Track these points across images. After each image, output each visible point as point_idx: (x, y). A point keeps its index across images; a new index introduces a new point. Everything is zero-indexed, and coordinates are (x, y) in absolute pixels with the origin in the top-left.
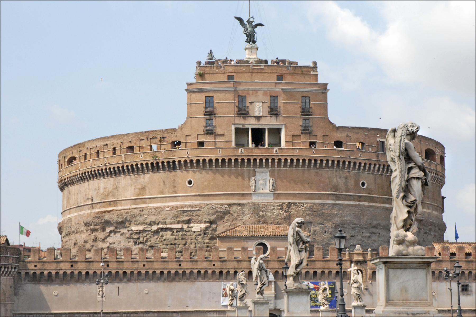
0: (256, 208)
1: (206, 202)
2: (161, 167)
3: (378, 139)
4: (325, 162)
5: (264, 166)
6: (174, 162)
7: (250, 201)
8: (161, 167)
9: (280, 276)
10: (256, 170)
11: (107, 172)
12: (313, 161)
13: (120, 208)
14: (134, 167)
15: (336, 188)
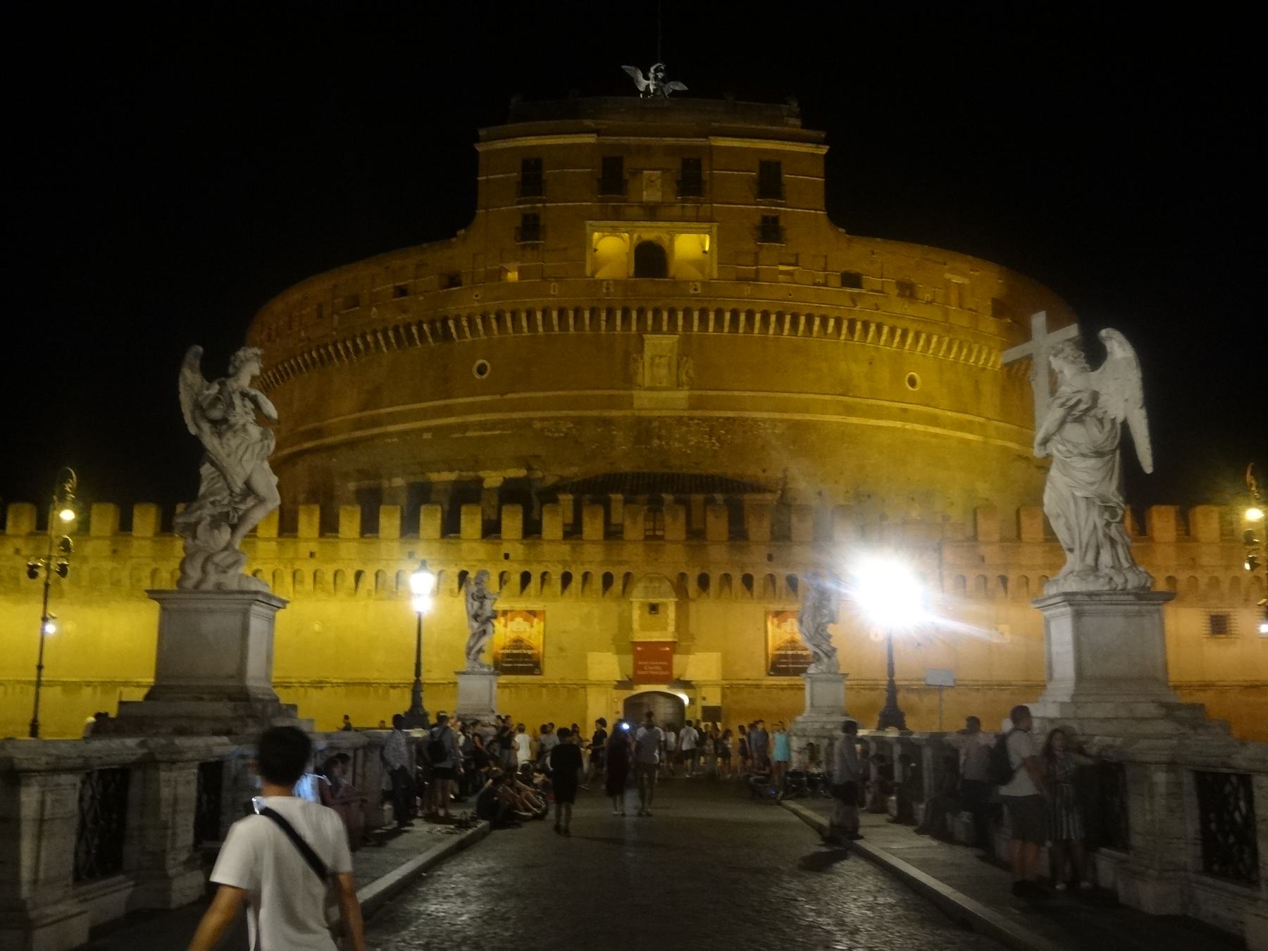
0: (643, 429)
1: (515, 415)
2: (416, 336)
3: (948, 276)
4: (817, 322)
5: (665, 328)
6: (445, 321)
7: (628, 413)
8: (416, 336)
9: (692, 586)
10: (647, 336)
11: (305, 361)
12: (788, 318)
13: (329, 440)
14: (359, 341)
15: (846, 388)
